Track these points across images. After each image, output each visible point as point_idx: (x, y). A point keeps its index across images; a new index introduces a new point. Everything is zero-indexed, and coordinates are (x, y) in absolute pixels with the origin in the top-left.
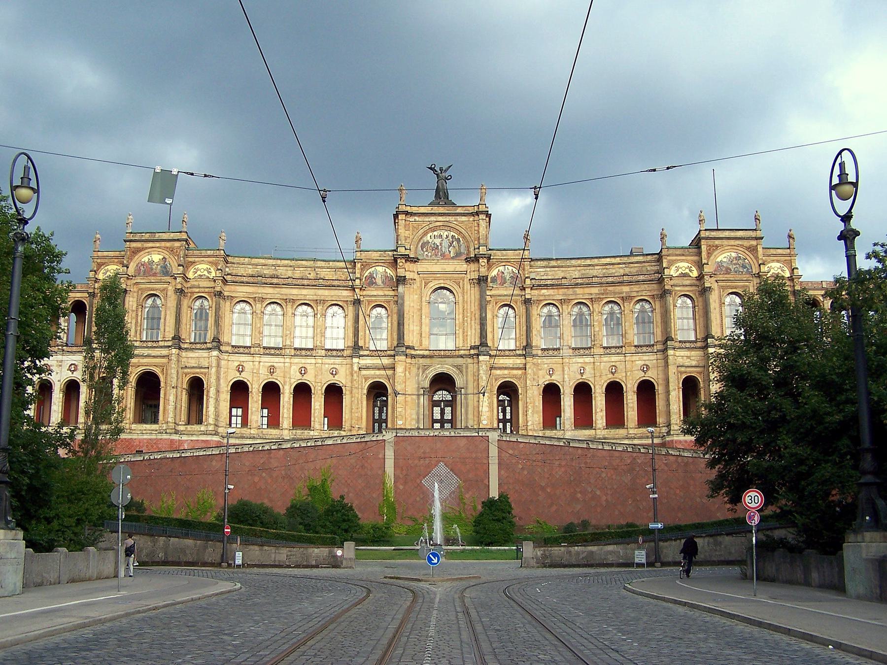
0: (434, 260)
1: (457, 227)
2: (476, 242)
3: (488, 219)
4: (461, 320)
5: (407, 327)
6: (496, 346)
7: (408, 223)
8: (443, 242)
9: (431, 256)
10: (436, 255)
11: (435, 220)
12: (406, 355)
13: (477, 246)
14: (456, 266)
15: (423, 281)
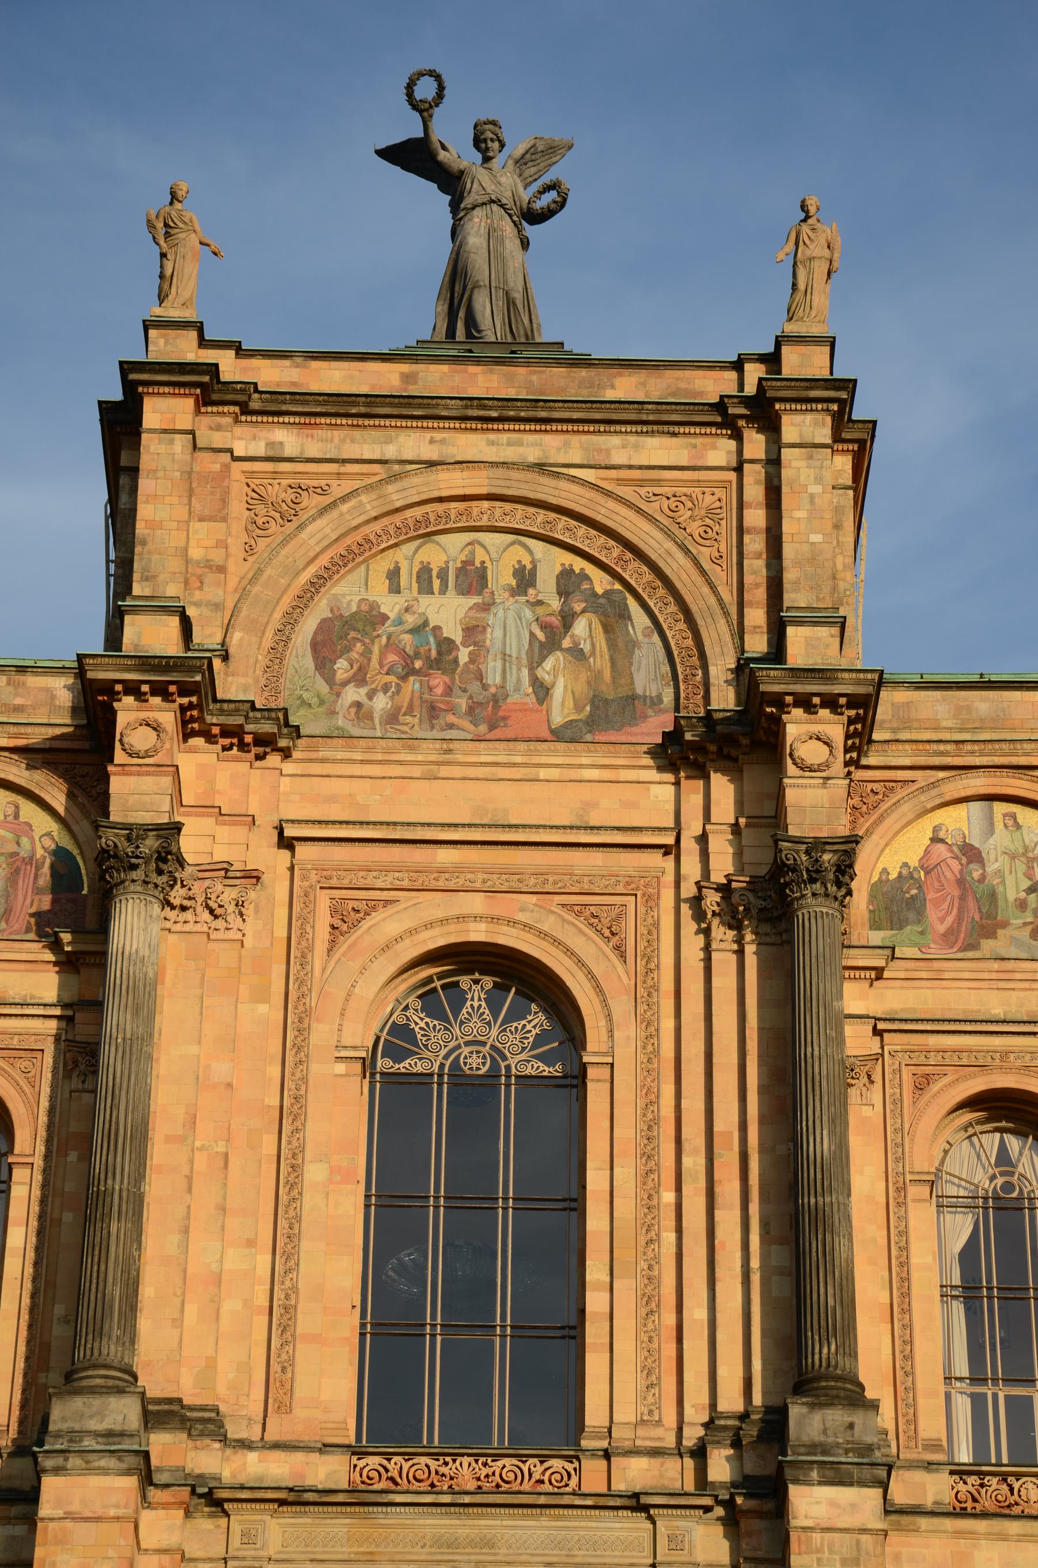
0: (411, 742)
1: (605, 511)
2: (757, 616)
3: (843, 463)
4: (625, 1208)
5: (174, 1240)
6: (931, 1426)
7: (213, 464)
8: (494, 619)
9: (392, 718)
10: (433, 712)
11: (430, 453)
12: (147, 1477)
13: (757, 644)
14: (585, 792)
15: (324, 901)
